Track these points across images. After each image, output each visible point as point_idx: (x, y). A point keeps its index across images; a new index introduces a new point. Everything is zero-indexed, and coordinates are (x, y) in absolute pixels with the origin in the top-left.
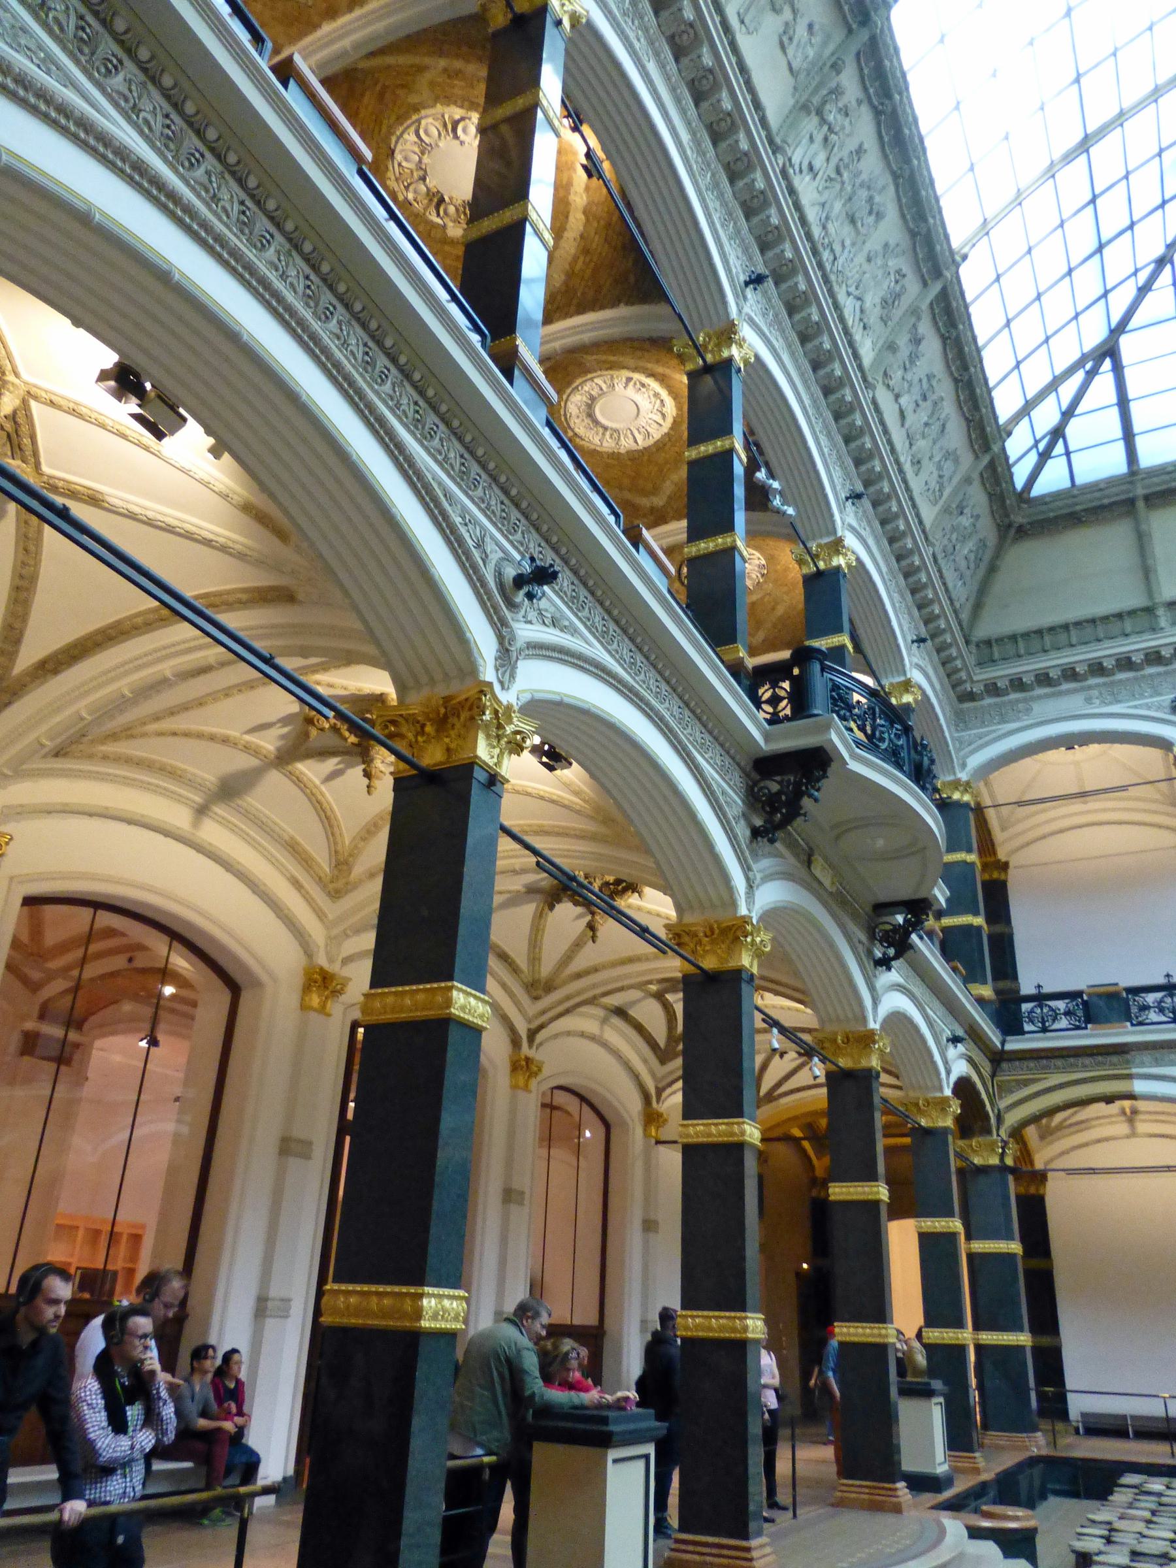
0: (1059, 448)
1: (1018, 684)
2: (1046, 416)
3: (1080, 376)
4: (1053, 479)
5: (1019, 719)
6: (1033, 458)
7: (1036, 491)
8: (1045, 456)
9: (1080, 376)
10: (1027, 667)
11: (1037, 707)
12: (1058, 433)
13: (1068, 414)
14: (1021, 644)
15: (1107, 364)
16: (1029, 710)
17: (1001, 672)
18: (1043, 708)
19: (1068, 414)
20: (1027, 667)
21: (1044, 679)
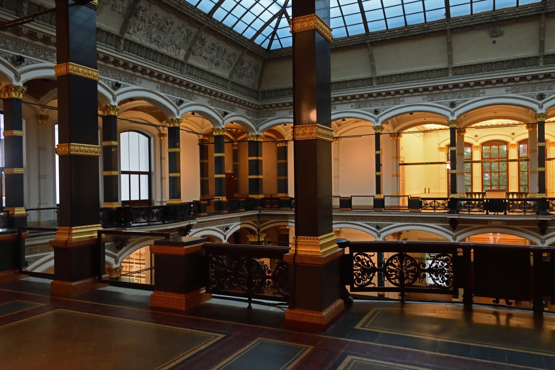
0: (276, 37)
1: (271, 106)
2: (268, 31)
3: (276, 19)
4: (276, 45)
5: (272, 116)
6: (268, 41)
7: (272, 48)
8: (272, 40)
9: (276, 19)
10: (274, 102)
11: (277, 113)
12: (274, 33)
13: (276, 28)
14: (273, 93)
15: (284, 16)
16: (275, 114)
17: (267, 103)
18: (279, 114)
19: (276, 28)
20: (274, 102)
21: (277, 105)
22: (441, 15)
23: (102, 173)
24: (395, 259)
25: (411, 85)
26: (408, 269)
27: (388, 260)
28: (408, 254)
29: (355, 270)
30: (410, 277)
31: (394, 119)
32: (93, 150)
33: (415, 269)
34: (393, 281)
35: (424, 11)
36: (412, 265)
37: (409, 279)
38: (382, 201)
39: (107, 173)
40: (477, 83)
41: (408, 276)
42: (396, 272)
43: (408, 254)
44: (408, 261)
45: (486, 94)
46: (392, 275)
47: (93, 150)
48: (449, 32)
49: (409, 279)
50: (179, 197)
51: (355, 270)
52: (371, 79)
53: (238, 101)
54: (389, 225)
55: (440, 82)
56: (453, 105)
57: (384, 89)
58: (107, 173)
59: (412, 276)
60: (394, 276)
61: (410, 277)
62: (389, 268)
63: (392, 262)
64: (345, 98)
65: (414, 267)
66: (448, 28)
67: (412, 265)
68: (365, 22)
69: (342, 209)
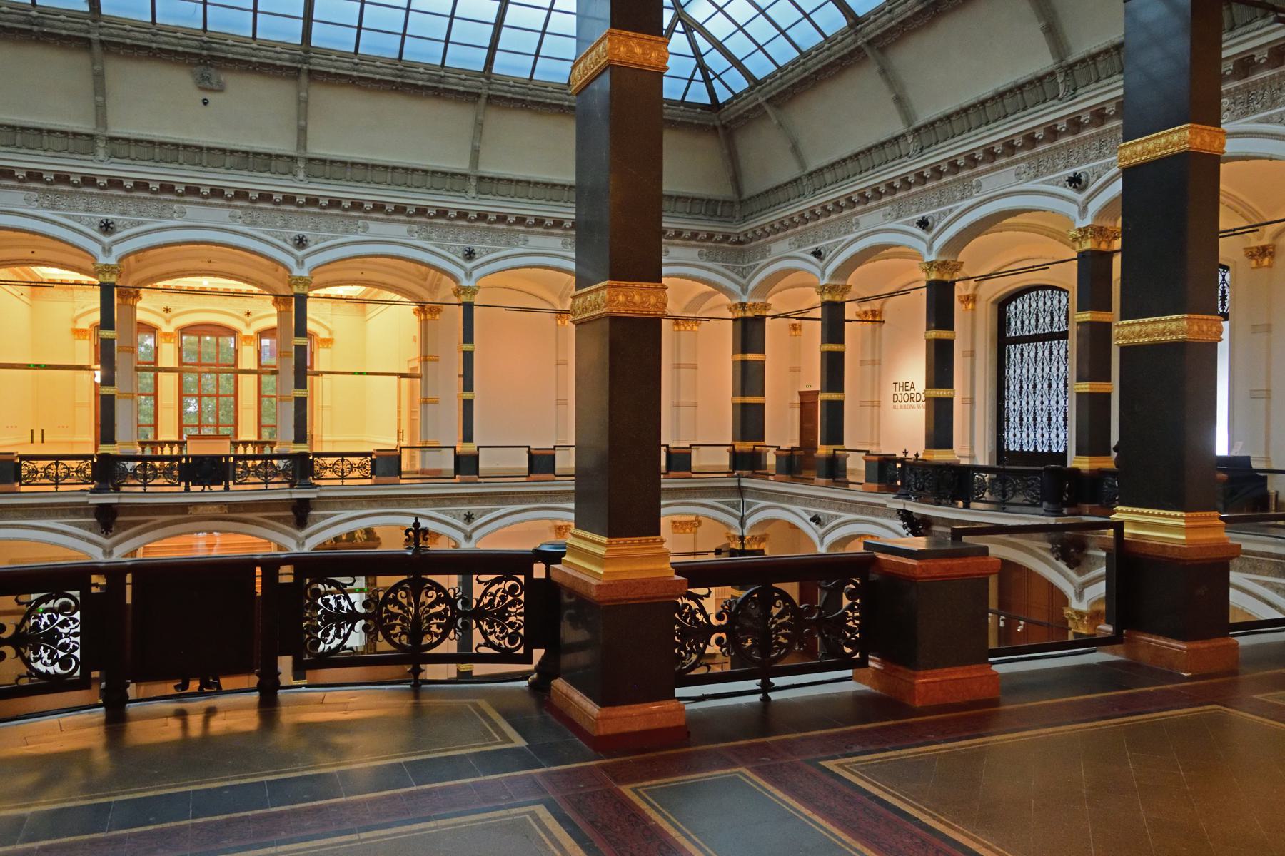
22: (476, 60)
23: (1114, 387)
24: (404, 589)
25: (391, 196)
26: (432, 611)
27: (386, 595)
28: (430, 577)
29: (520, 614)
30: (434, 628)
31: (432, 271)
32: (1128, 332)
33: (445, 610)
34: (396, 640)
35: (447, 41)
36: (438, 601)
37: (431, 633)
38: (474, 458)
39: (1099, 387)
40: (521, 220)
41: (429, 627)
42: (404, 619)
43: (430, 577)
44: (430, 594)
45: (530, 243)
46: (394, 627)
47: (1128, 332)
48: (483, 100)
49: (431, 633)
50: (948, 445)
51: (520, 614)
52: (292, 158)
53: (777, 226)
54: (492, 511)
55: (453, 202)
56: (470, 255)
57: (491, 205)
58: (1099, 387)
59: (439, 626)
60: (398, 629)
61: (434, 628)
62: (387, 611)
63: (395, 598)
64: (217, 192)
65: (443, 606)
66: (485, 91)
67: (438, 601)
68: (308, 18)
69: (533, 476)
